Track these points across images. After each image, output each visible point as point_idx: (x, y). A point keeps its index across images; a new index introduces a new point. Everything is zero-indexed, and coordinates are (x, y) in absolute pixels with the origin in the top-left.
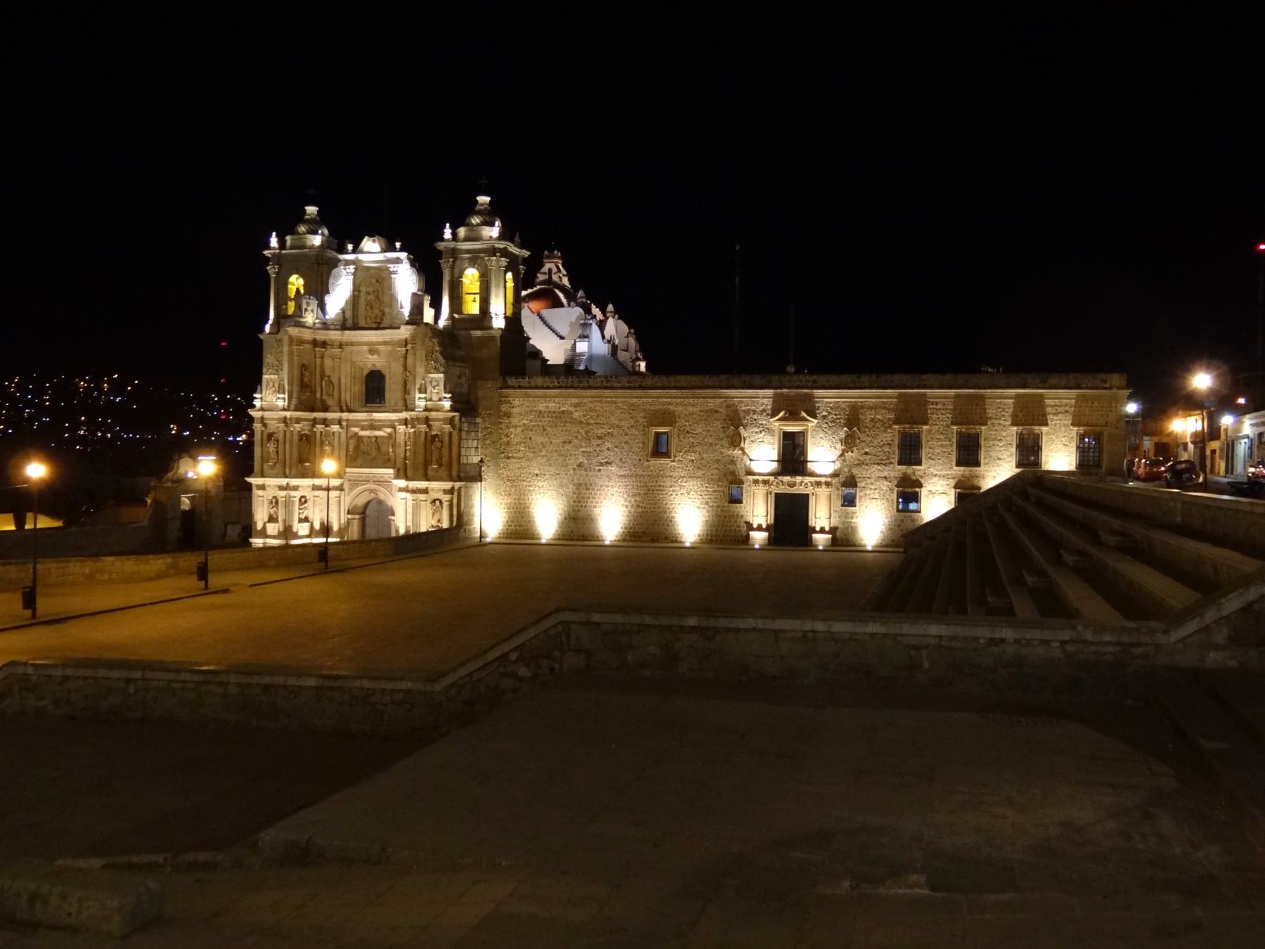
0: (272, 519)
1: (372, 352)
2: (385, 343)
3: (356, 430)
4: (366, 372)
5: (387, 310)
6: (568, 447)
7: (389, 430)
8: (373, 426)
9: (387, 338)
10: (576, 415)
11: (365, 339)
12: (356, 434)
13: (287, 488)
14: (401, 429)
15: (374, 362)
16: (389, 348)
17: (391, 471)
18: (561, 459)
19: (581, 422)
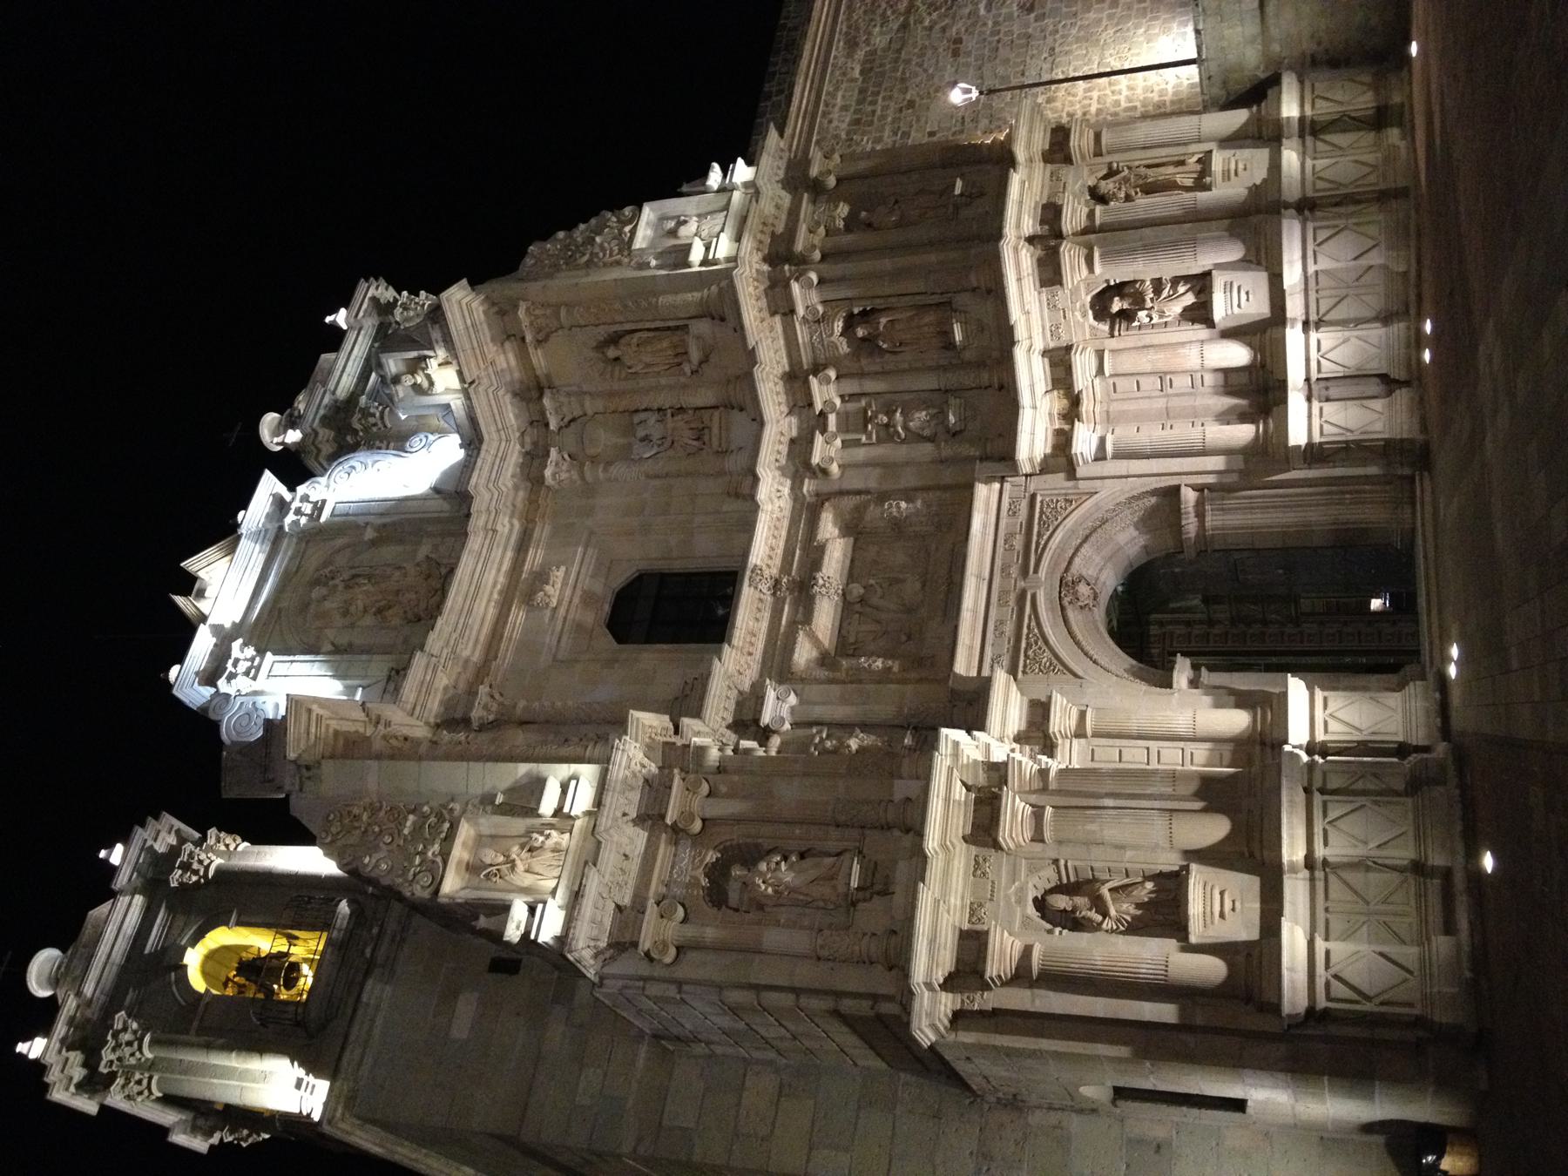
0: (1164, 912)
1: (541, 577)
2: (522, 548)
3: (804, 653)
4: (606, 641)
5: (424, 550)
6: (970, 43)
7: (828, 527)
8: (799, 588)
9: (508, 527)
10: (880, 40)
11: (485, 610)
12: (825, 660)
13: (984, 827)
14: (823, 450)
15: (571, 586)
16: (542, 532)
17: (985, 495)
18: (1003, 52)
19: (904, 26)
